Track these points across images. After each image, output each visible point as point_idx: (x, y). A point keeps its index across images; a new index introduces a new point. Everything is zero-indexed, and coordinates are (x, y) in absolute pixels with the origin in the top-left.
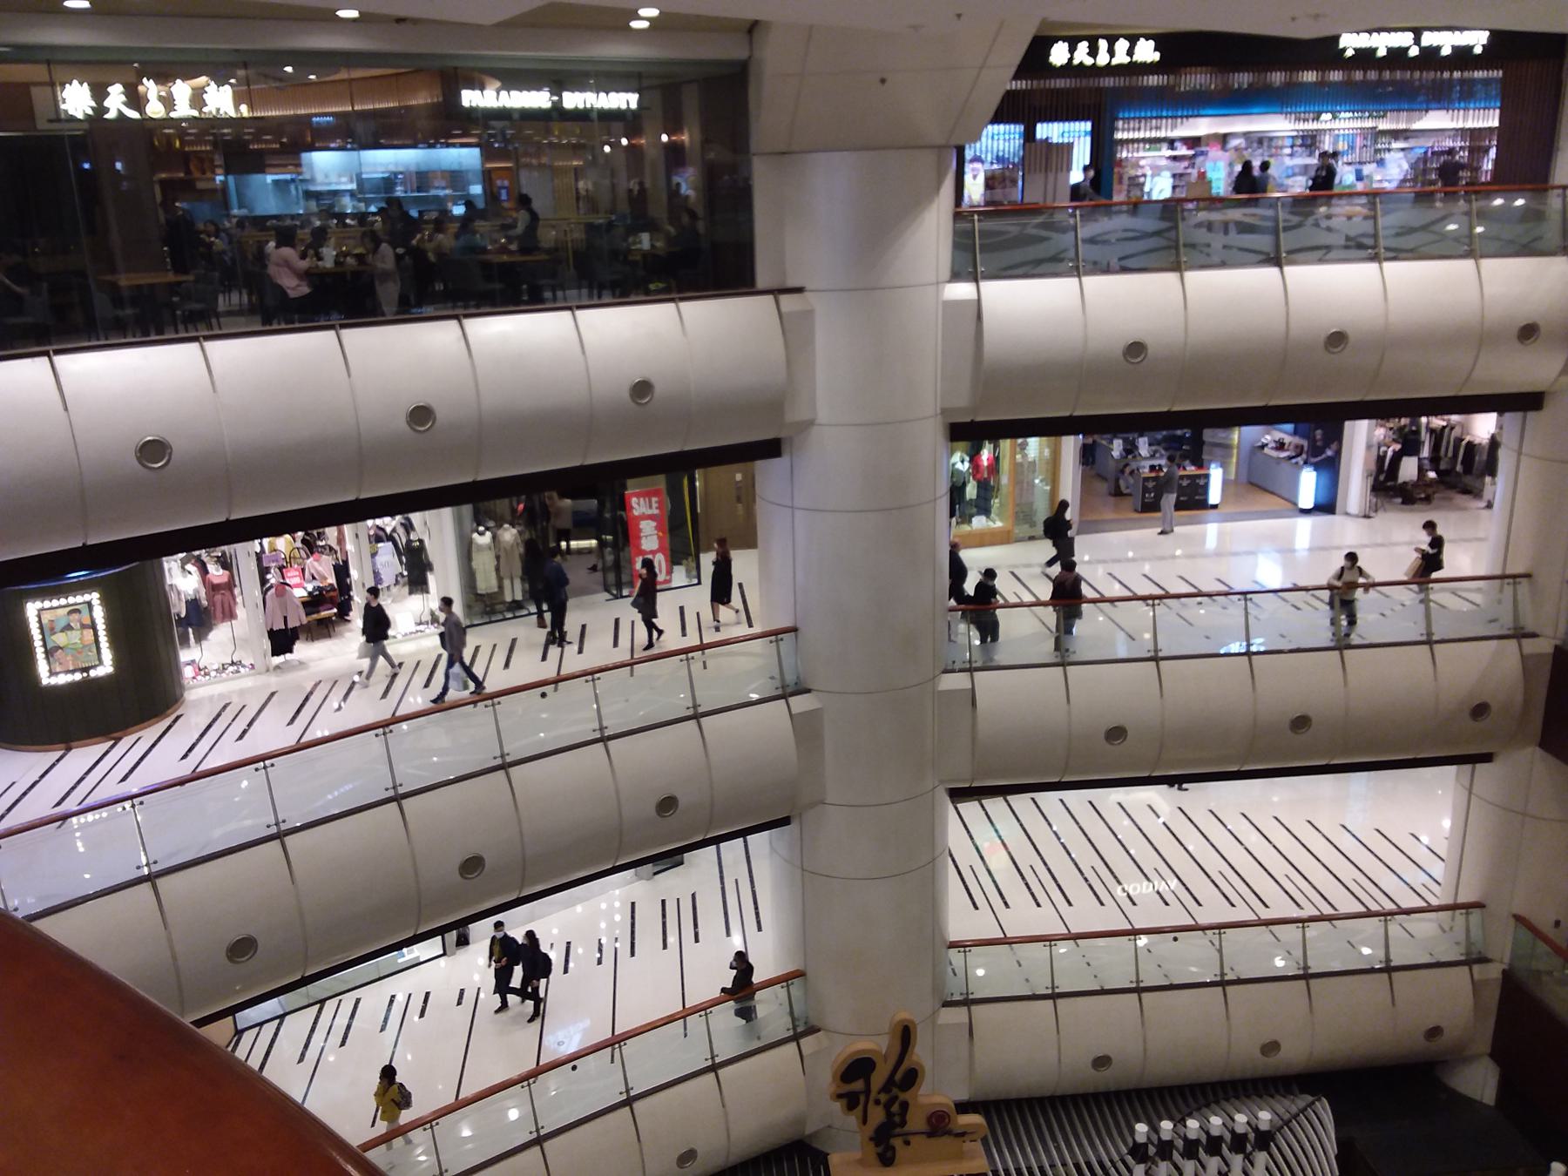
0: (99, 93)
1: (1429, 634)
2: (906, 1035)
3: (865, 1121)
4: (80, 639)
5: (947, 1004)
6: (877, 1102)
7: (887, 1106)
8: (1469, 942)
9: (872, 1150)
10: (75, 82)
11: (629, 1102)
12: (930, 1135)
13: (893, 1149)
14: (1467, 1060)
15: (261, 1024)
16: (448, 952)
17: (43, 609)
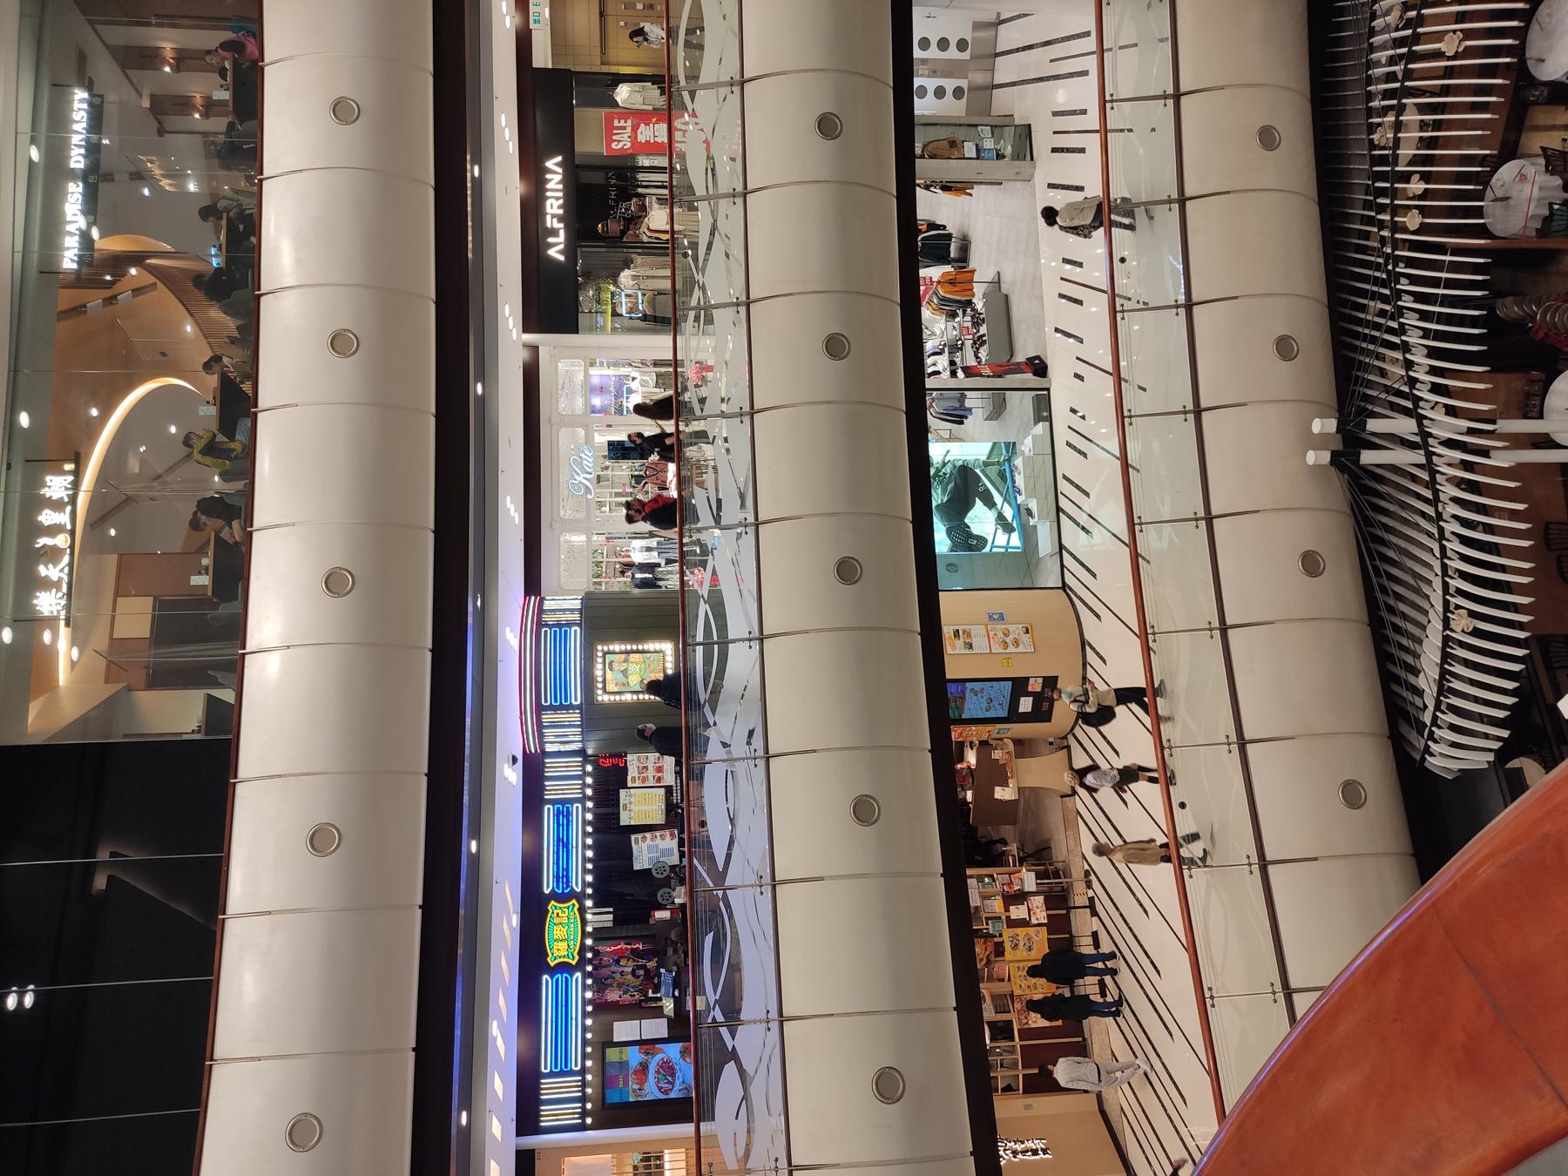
0: (47, 584)
4: (637, 664)
10: (35, 602)
15: (1062, 566)
16: (1047, 386)
17: (604, 688)
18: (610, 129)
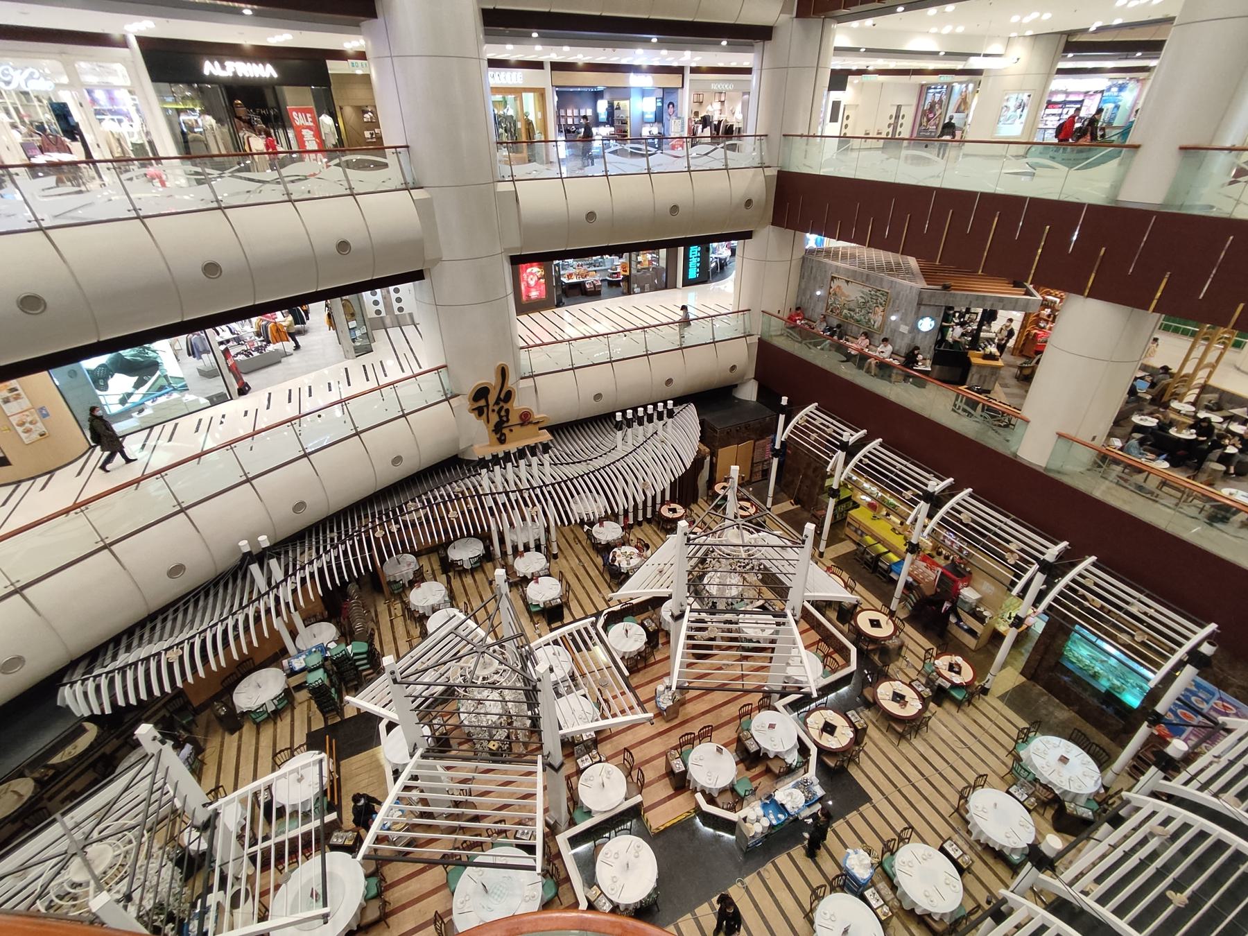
1: (726, 165)
2: (503, 372)
3: (488, 422)
5: (522, 378)
6: (493, 411)
7: (499, 412)
8: (745, 329)
9: (495, 437)
11: (357, 434)
12: (522, 425)
13: (504, 434)
14: (744, 383)
18: (304, 111)
